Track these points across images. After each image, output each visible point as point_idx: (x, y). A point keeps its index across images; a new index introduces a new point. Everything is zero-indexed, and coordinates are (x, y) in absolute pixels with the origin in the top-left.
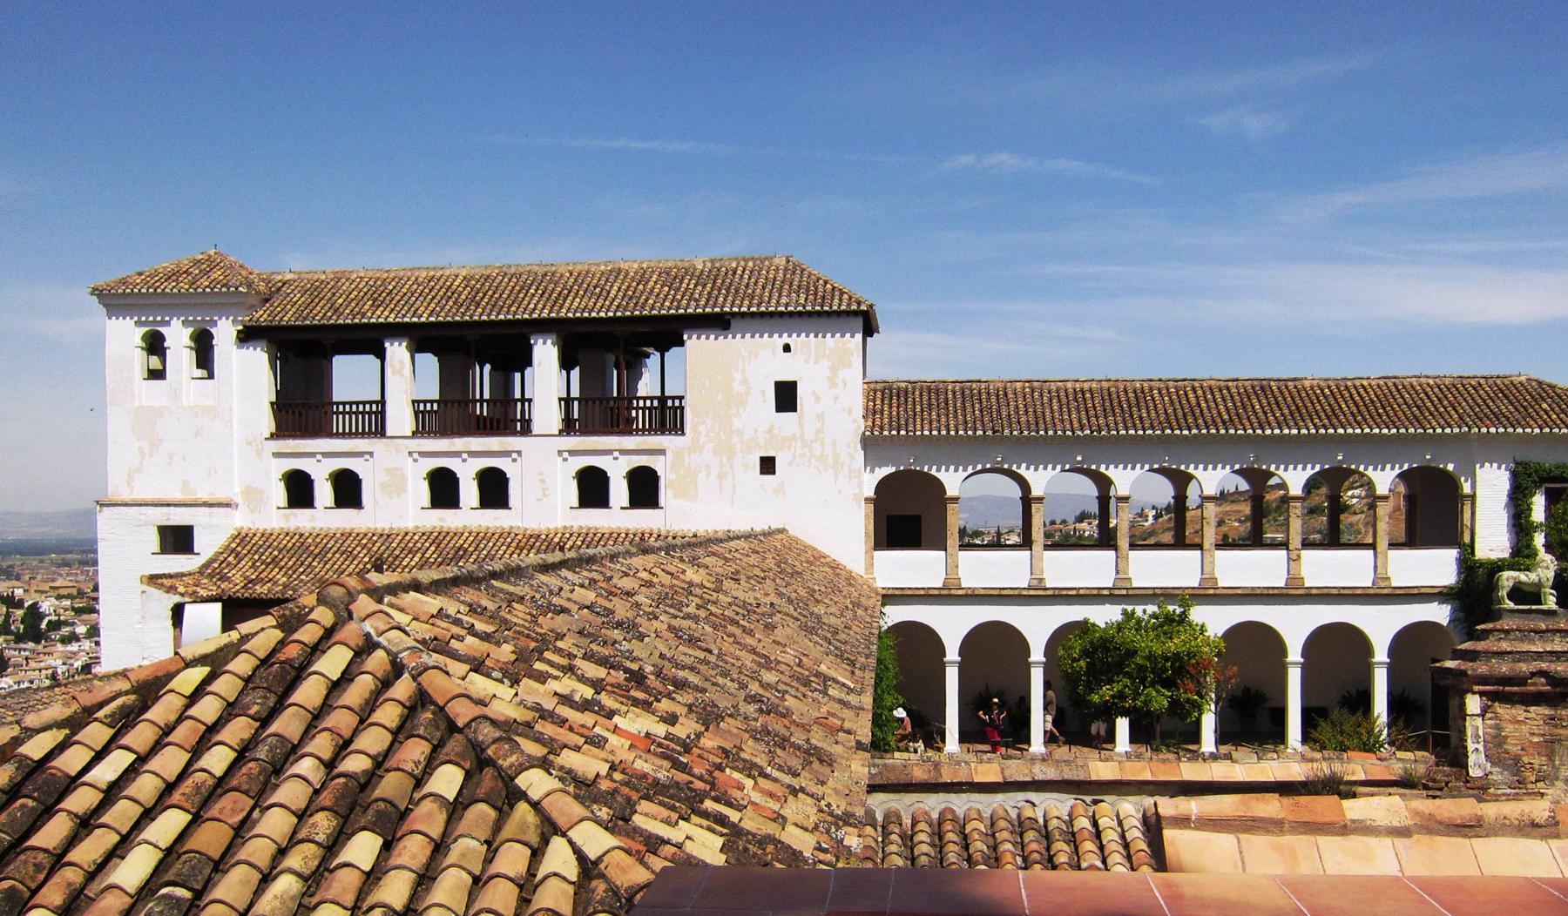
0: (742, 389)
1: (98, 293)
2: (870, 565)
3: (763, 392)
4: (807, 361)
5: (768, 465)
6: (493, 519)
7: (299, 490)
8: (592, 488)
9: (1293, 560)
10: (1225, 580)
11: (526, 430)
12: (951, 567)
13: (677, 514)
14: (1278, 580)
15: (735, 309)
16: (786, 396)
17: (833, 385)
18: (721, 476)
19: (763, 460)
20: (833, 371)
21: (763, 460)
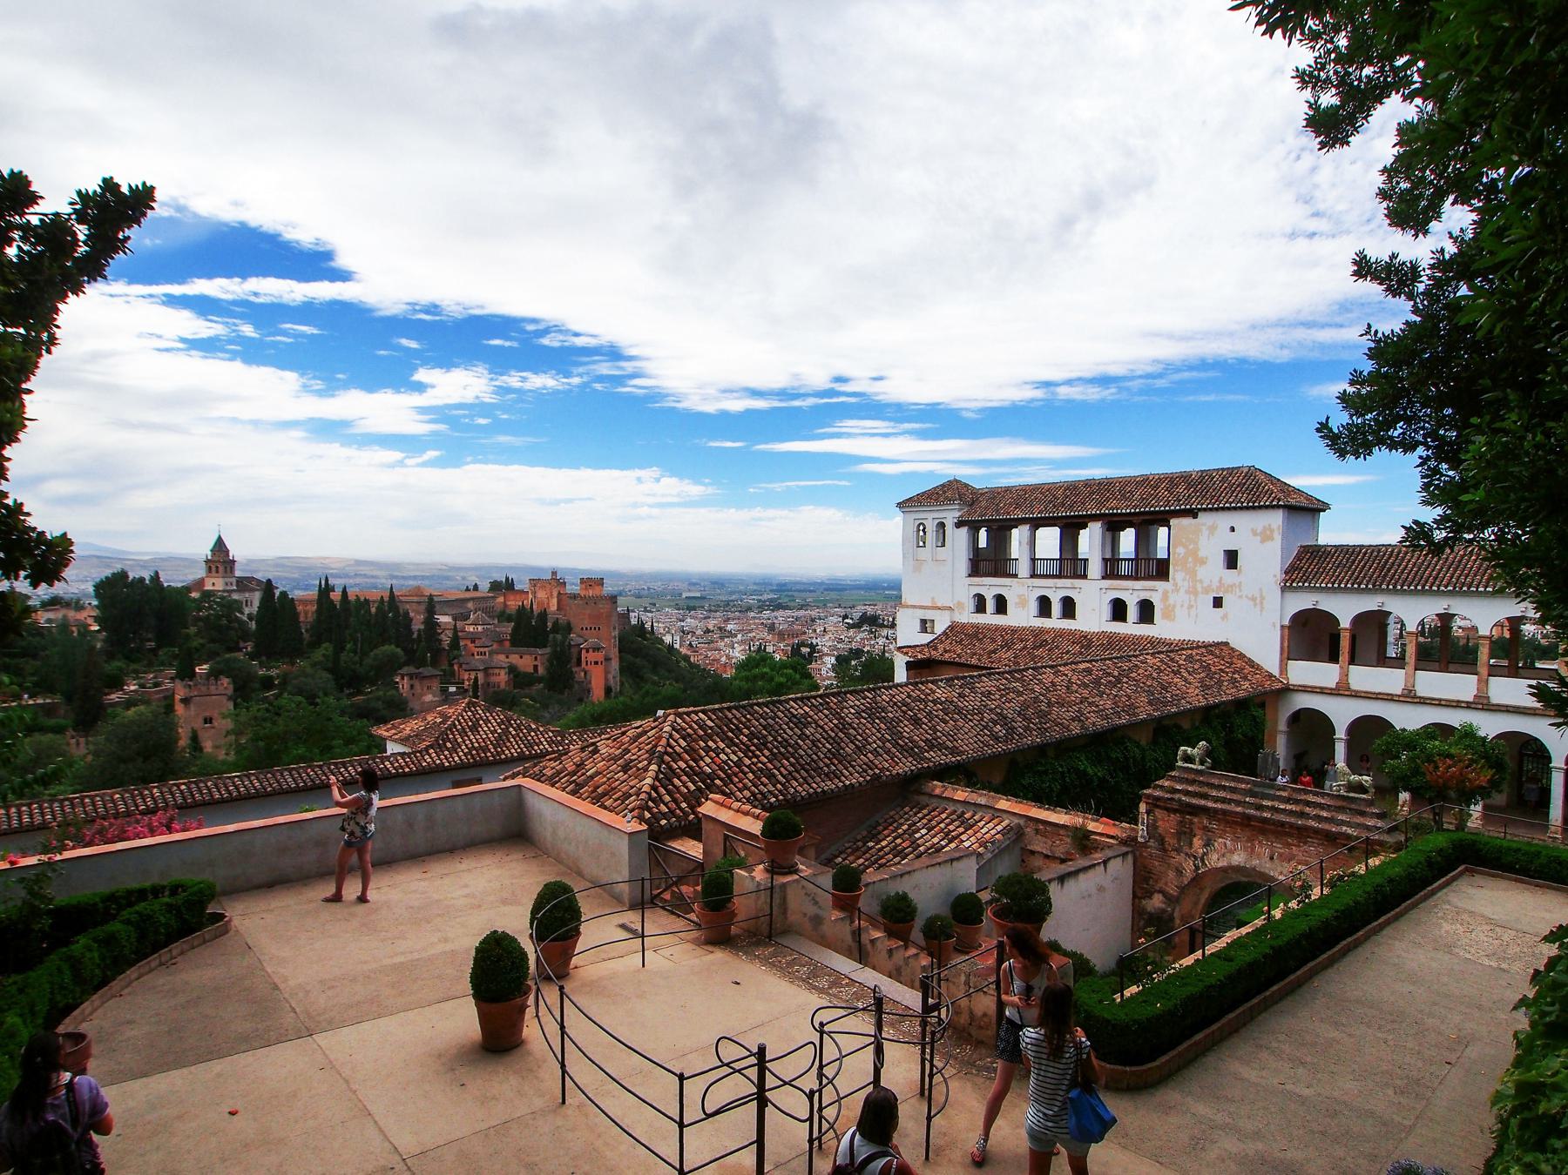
1: (900, 505)
2: (1283, 669)
5: (1218, 602)
6: (1067, 624)
7: (980, 605)
11: (1085, 577)
16: (1232, 559)
18: (1190, 607)
20: (1262, 540)
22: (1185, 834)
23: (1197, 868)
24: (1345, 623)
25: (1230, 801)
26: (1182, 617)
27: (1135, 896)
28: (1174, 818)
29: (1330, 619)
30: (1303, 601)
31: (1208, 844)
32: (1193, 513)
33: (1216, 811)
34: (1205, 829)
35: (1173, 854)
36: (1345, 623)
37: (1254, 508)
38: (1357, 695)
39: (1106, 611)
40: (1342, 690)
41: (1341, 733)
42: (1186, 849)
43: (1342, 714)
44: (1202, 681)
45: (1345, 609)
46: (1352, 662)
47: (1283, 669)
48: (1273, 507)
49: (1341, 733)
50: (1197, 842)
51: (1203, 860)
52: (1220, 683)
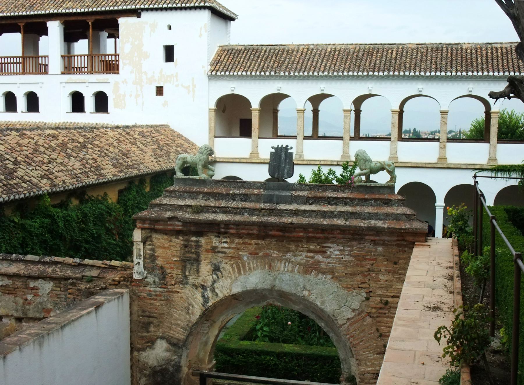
5: (160, 91)
6: (32, 118)
8: (77, 102)
9: (443, 148)
10: (402, 158)
11: (46, 72)
12: (255, 147)
13: (116, 116)
14: (433, 159)
15: (142, 7)
16: (169, 53)
19: (157, 87)
21: (157, 87)
22: (190, 260)
23: (206, 300)
24: (255, 105)
25: (241, 211)
26: (132, 105)
27: (133, 349)
28: (178, 241)
31: (216, 269)
32: (136, 13)
33: (227, 224)
34: (214, 250)
35: (177, 288)
36: (255, 105)
39: (68, 103)
42: (191, 280)
44: (154, 150)
45: (254, 92)
48: (200, 8)
50: (205, 268)
51: (213, 290)
52: (168, 154)
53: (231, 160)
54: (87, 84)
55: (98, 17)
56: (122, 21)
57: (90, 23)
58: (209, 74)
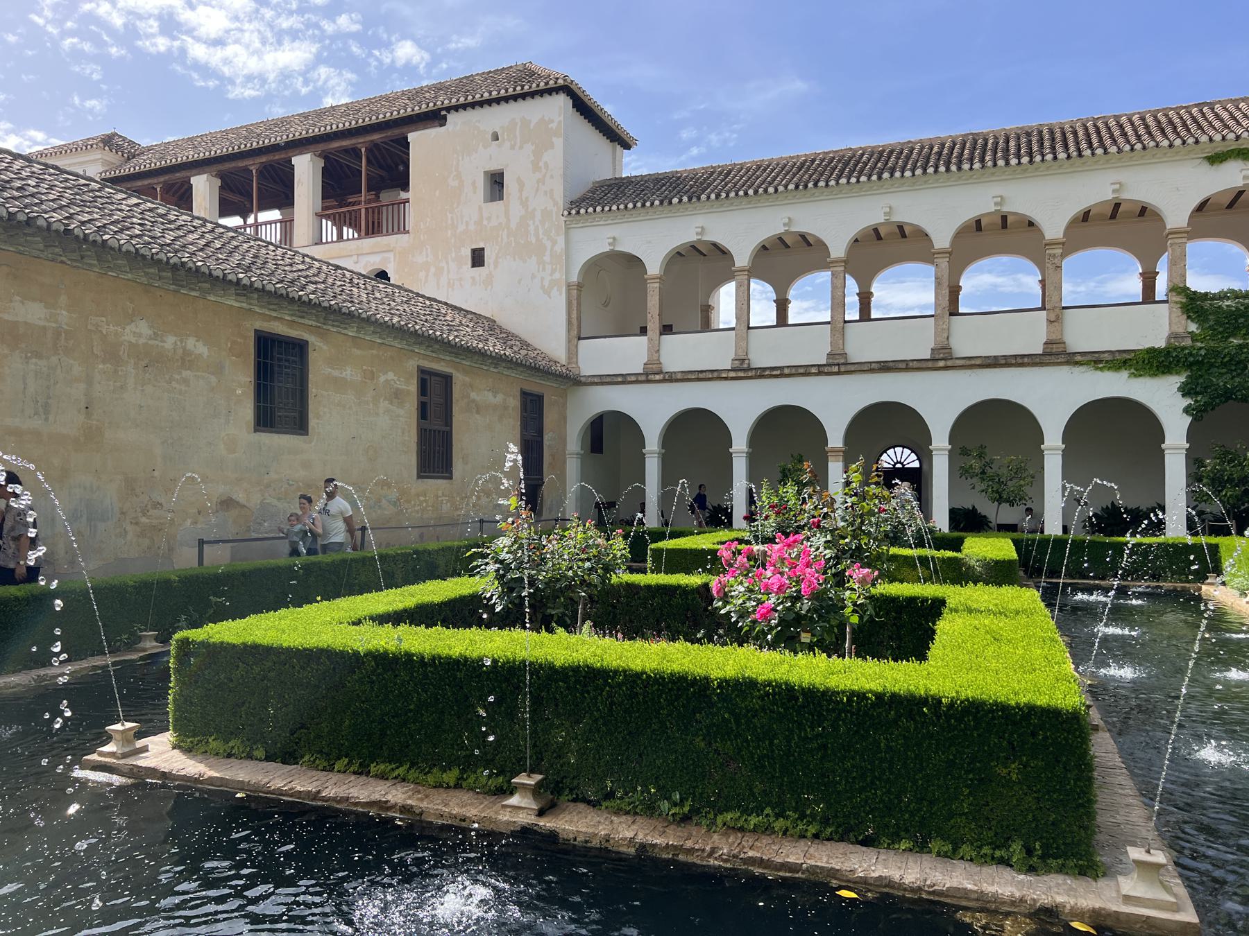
0: (455, 183)
2: (572, 353)
3: (474, 183)
4: (512, 147)
5: (478, 258)
12: (655, 350)
17: (536, 168)
19: (474, 251)
21: (474, 251)
24: (654, 267)
29: (633, 262)
30: (597, 238)
36: (654, 267)
37: (523, 96)
38: (671, 378)
40: (653, 375)
41: (652, 443)
43: (653, 411)
46: (667, 329)
47: (572, 353)
49: (652, 443)
53: (608, 380)
54: (355, 258)
55: (376, 137)
56: (417, 139)
57: (363, 150)
58: (566, 213)
